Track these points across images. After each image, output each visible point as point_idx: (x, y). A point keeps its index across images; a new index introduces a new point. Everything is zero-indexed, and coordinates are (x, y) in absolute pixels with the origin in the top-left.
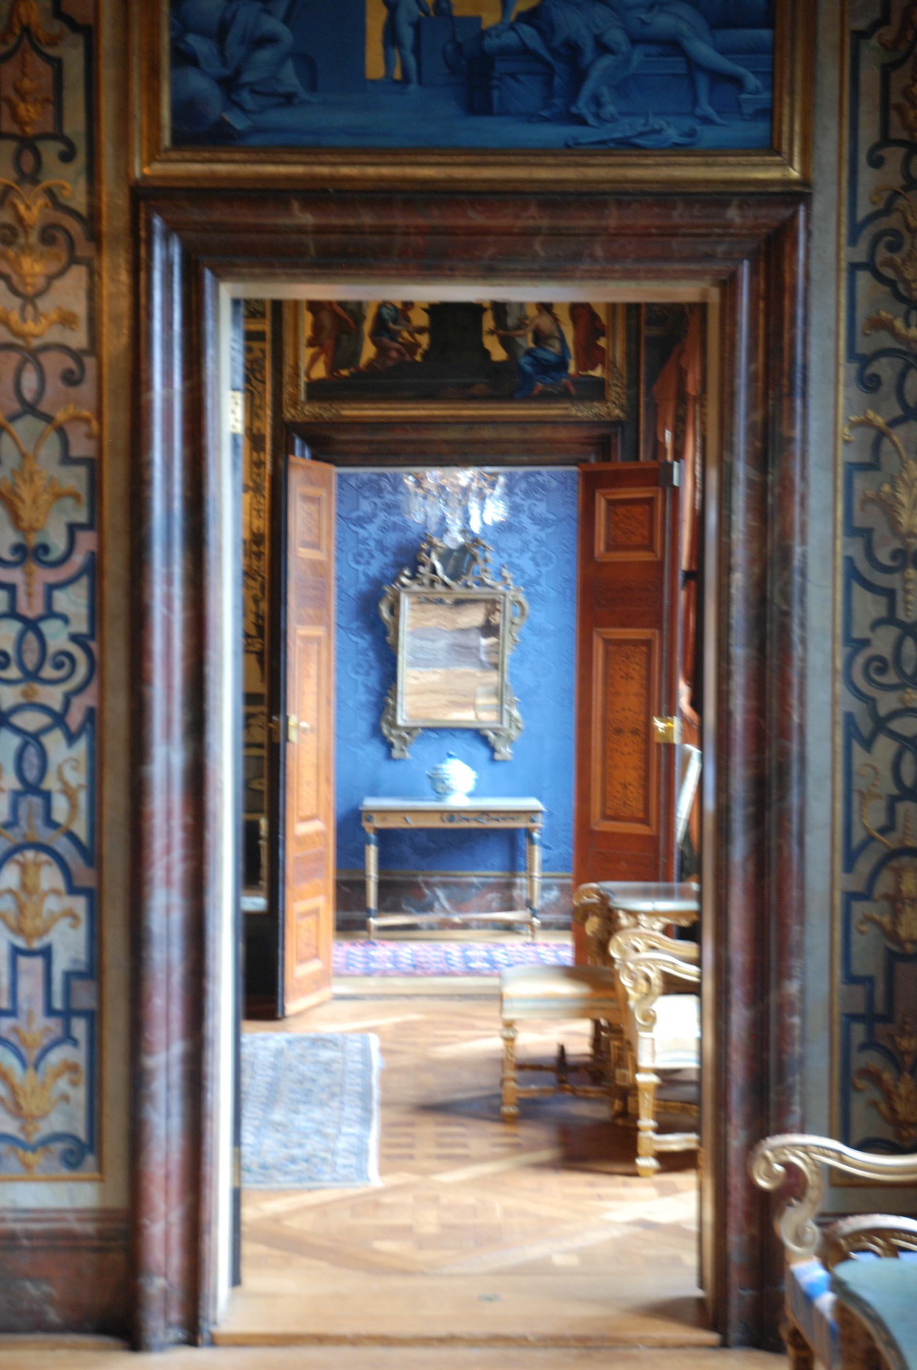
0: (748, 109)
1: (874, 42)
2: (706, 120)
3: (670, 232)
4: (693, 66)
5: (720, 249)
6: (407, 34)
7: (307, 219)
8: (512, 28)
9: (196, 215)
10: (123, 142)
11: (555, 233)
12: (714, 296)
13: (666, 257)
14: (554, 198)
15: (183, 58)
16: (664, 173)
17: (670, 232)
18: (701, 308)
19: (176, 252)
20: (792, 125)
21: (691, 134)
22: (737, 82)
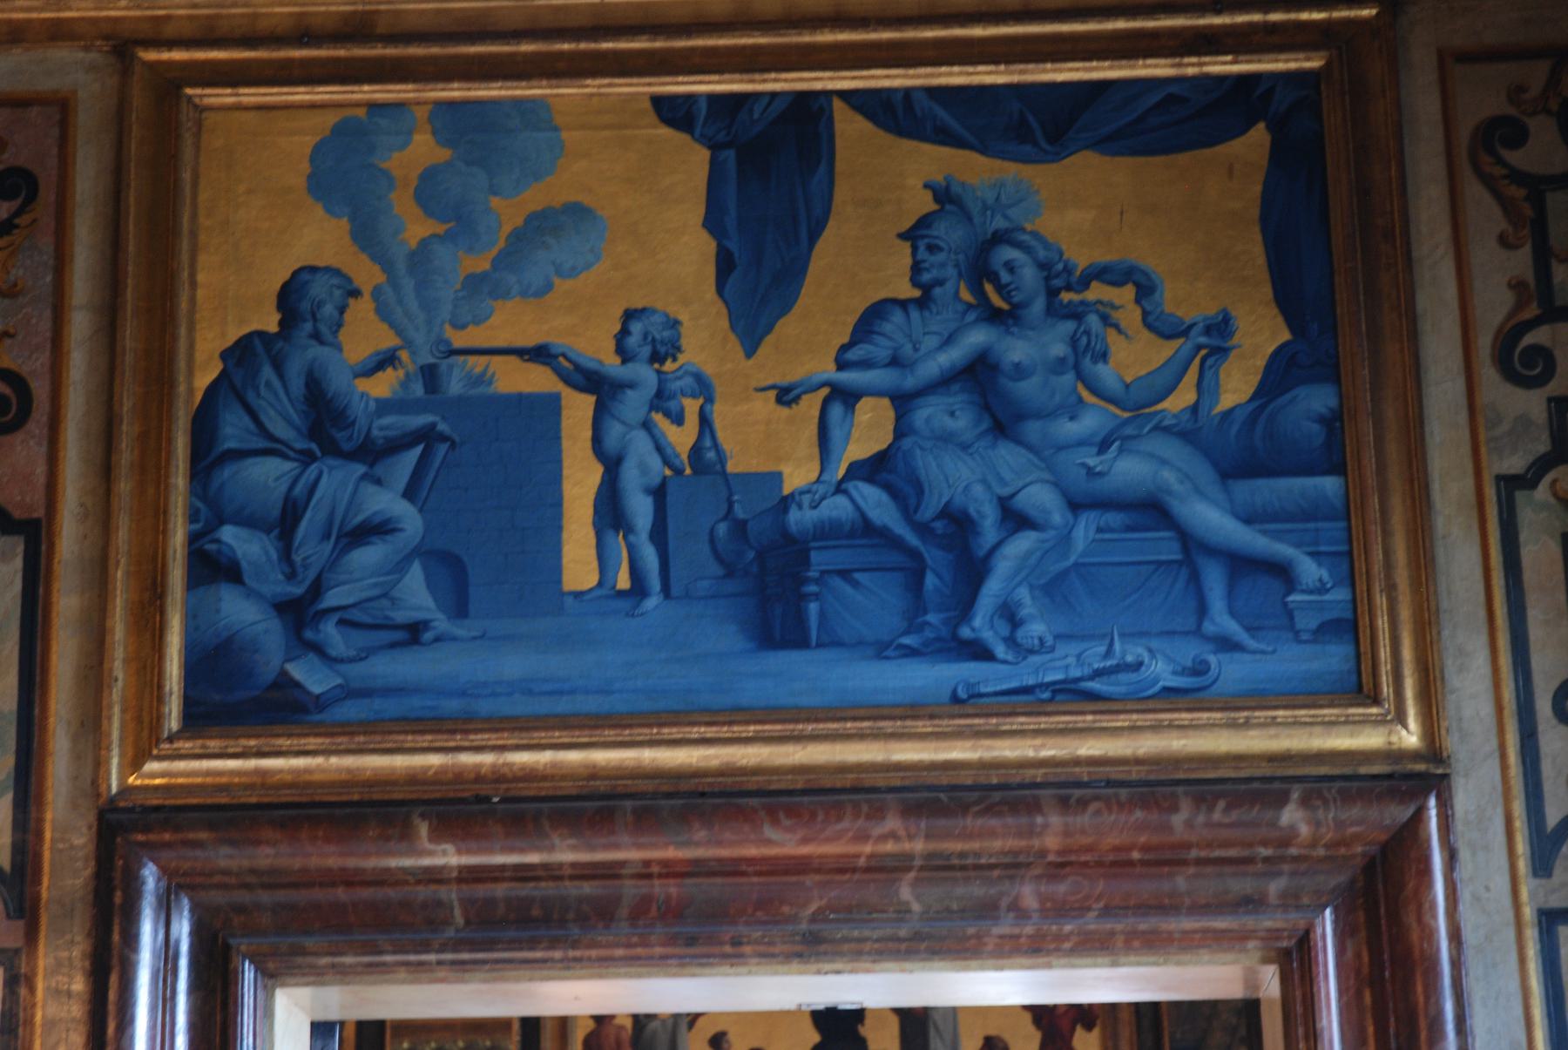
0: (1307, 622)
1: (1542, 492)
2: (1227, 645)
3: (1167, 859)
4: (1192, 546)
5: (1274, 887)
6: (641, 509)
7: (449, 857)
8: (839, 489)
9: (226, 858)
10: (91, 724)
11: (938, 867)
12: (1270, 983)
13: (1166, 907)
14: (932, 797)
15: (211, 568)
16: (1148, 745)
17: (1167, 859)
18: (1250, 1009)
19: (183, 929)
20: (1396, 651)
21: (1200, 669)
22: (1282, 572)
